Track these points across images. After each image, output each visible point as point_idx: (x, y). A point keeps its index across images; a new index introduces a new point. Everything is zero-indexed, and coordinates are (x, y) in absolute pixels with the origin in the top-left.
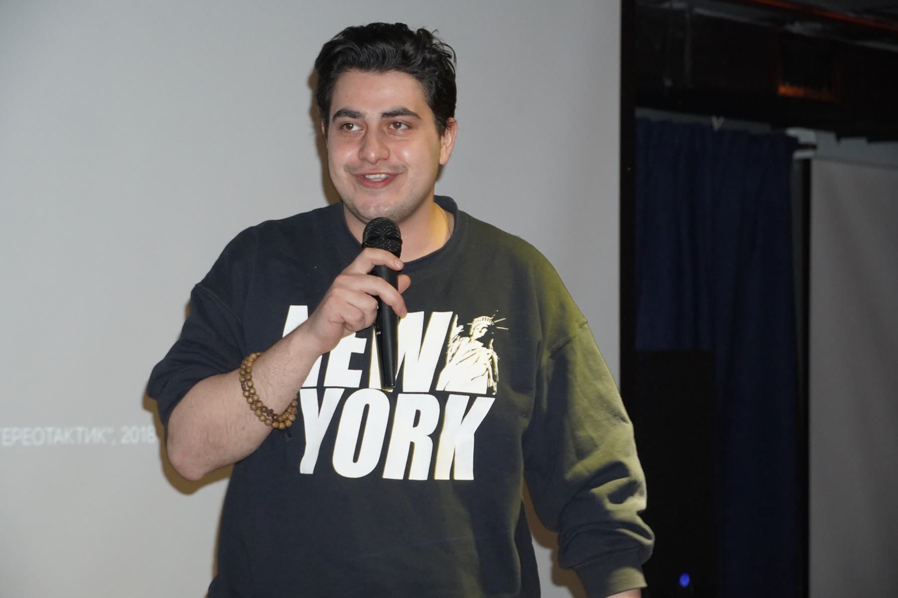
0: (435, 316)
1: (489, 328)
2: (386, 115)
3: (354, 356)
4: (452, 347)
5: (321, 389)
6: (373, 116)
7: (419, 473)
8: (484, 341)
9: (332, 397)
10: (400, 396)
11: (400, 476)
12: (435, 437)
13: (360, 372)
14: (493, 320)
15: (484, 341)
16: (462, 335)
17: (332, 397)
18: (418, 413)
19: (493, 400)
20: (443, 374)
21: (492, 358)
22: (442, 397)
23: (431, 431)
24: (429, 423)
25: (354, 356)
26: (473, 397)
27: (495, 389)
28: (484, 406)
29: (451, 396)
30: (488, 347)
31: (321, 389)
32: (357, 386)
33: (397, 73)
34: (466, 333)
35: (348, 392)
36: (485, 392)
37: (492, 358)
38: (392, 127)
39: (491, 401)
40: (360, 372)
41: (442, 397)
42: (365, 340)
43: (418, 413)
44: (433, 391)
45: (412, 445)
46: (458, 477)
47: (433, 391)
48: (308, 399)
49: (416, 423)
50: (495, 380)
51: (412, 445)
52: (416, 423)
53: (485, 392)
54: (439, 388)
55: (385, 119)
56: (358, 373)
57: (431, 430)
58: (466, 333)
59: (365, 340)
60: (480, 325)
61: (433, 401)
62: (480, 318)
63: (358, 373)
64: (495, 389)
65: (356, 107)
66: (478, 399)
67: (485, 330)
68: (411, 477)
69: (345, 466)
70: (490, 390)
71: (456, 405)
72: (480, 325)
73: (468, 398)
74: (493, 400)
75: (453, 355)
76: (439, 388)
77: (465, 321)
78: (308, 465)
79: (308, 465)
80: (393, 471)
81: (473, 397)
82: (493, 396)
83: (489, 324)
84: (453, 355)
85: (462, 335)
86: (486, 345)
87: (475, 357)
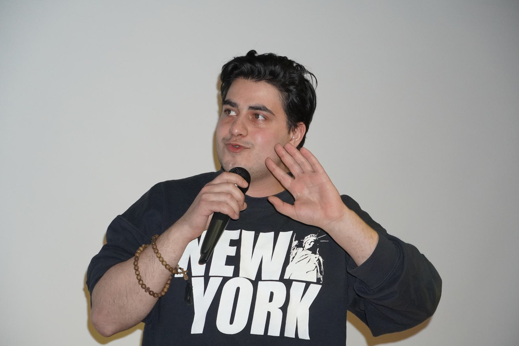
0: (282, 234)
1: (315, 241)
3: (228, 257)
4: (293, 252)
5: (207, 277)
9: (214, 284)
10: (260, 283)
12: (284, 309)
13: (232, 267)
14: (317, 236)
15: (313, 250)
17: (214, 284)
18: (272, 294)
19: (320, 286)
20: (288, 269)
21: (319, 259)
22: (288, 283)
23: (281, 305)
25: (228, 257)
26: (308, 284)
27: (322, 279)
28: (315, 290)
29: (294, 283)
30: (316, 254)
31: (207, 277)
32: (232, 276)
33: (266, 83)
35: (225, 279)
37: (319, 259)
39: (319, 287)
40: (232, 267)
41: (288, 283)
42: (236, 247)
43: (272, 294)
44: (282, 279)
45: (269, 314)
47: (282, 279)
48: (197, 284)
49: (271, 300)
50: (321, 274)
51: (269, 314)
52: (271, 300)
53: (315, 281)
54: (286, 277)
57: (281, 304)
59: (236, 247)
61: (282, 287)
62: (309, 236)
64: (322, 279)
66: (311, 284)
67: (313, 243)
70: (318, 280)
71: (297, 289)
73: (304, 284)
74: (320, 286)
75: (293, 258)
76: (286, 277)
81: (308, 284)
82: (320, 284)
83: (315, 239)
84: (293, 258)
86: (314, 253)
87: (308, 259)
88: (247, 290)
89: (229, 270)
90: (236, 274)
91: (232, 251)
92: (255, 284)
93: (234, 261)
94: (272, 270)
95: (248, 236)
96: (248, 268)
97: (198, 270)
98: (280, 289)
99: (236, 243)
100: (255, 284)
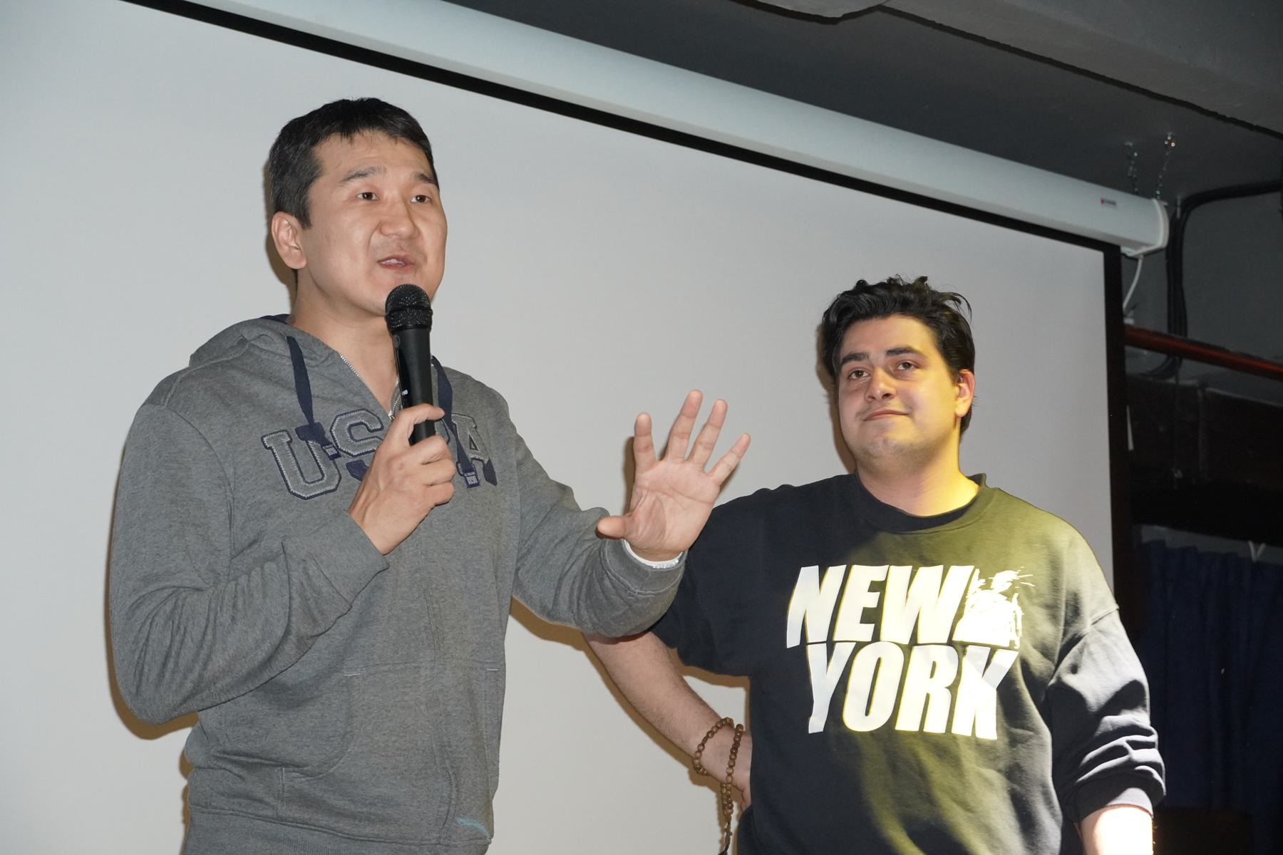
1: (1013, 582)
2: (891, 352)
3: (865, 610)
6: (878, 357)
7: (935, 726)
8: (1008, 595)
9: (842, 651)
11: (916, 728)
12: (953, 688)
13: (872, 626)
15: (1008, 595)
16: (982, 588)
17: (842, 651)
23: (949, 683)
24: (946, 674)
25: (865, 610)
31: (830, 644)
34: (987, 586)
35: (859, 646)
36: (1007, 645)
38: (901, 367)
40: (872, 626)
44: (950, 643)
45: (928, 696)
46: (979, 735)
47: (950, 643)
48: (816, 655)
51: (928, 696)
55: (891, 358)
56: (870, 628)
57: (950, 682)
58: (987, 586)
60: (1003, 579)
63: (870, 628)
65: (860, 348)
68: (926, 730)
69: (856, 720)
71: (975, 657)
78: (817, 723)
79: (817, 723)
80: (906, 723)
85: (982, 588)
88: (894, 659)
89: (866, 631)
90: (876, 637)
91: (871, 600)
92: (907, 649)
93: (872, 616)
94: (935, 630)
95: (898, 574)
96: (895, 627)
97: (817, 632)
98: (946, 657)
99: (878, 587)
100: (907, 649)
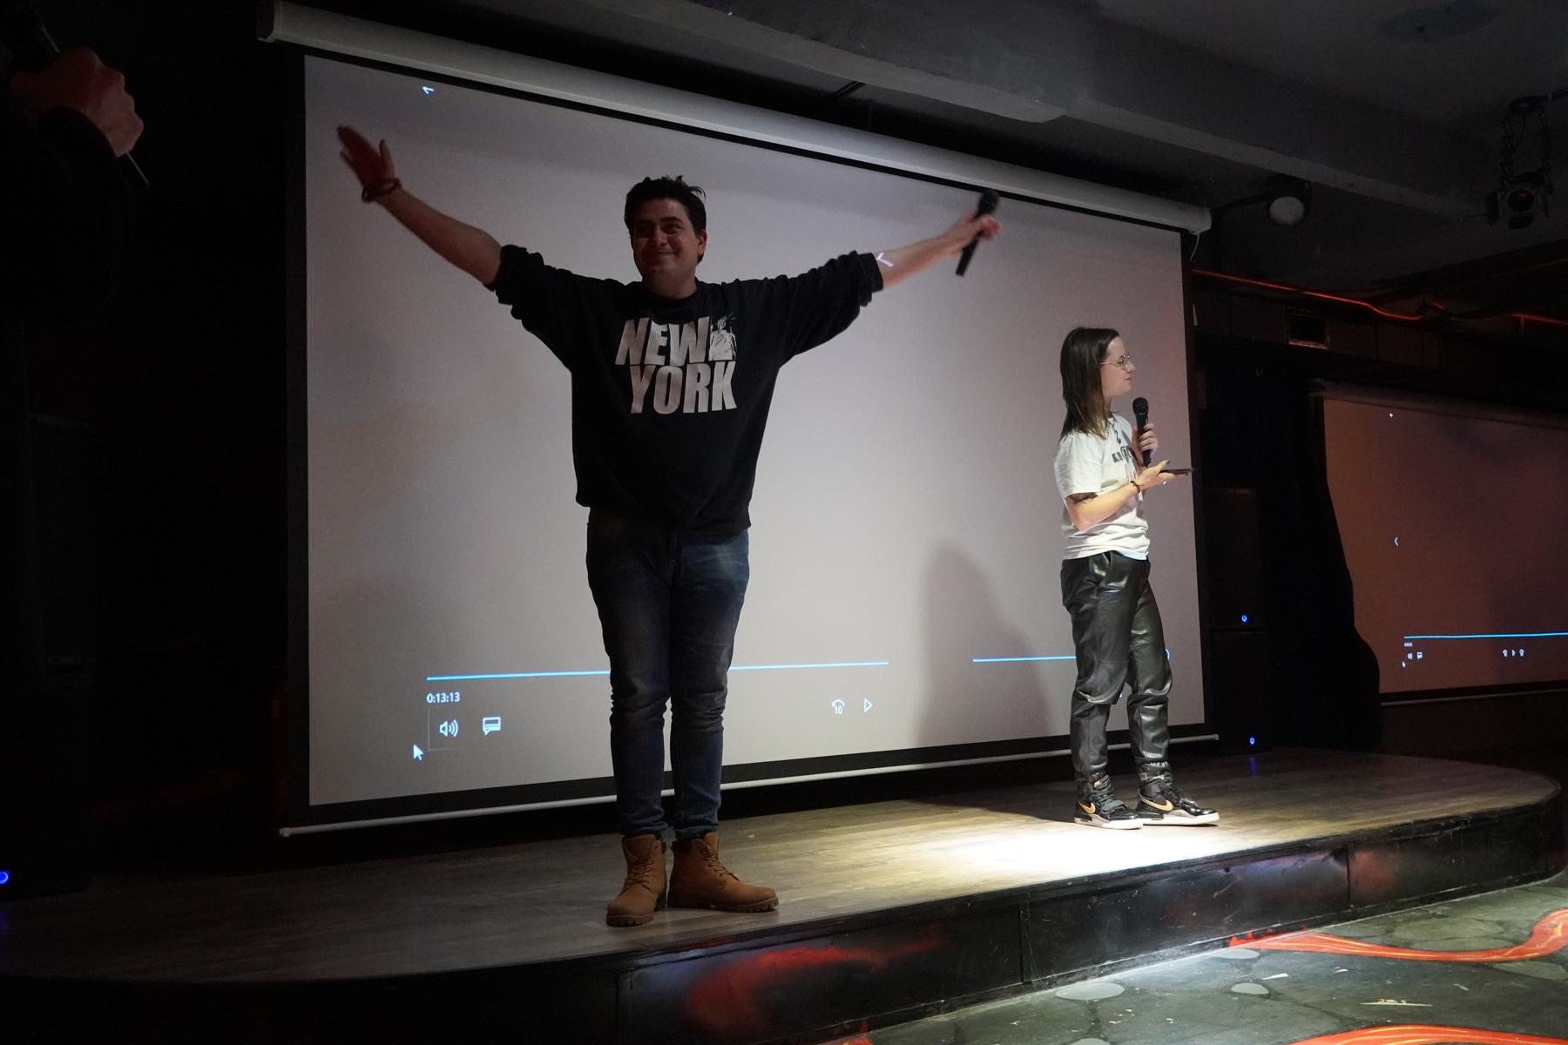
7: (703, 408)
12: (710, 387)
15: (727, 329)
22: (712, 364)
24: (705, 380)
26: (727, 362)
28: (732, 365)
34: (716, 329)
44: (706, 361)
58: (716, 329)
60: (721, 323)
61: (707, 367)
69: (659, 408)
71: (719, 367)
72: (721, 323)
77: (714, 322)
80: (688, 409)
81: (727, 362)
89: (660, 360)
90: (667, 362)
91: (663, 342)
92: (684, 368)
93: (664, 351)
95: (674, 328)
96: (676, 357)
98: (704, 370)
99: (666, 334)
100: (684, 368)
